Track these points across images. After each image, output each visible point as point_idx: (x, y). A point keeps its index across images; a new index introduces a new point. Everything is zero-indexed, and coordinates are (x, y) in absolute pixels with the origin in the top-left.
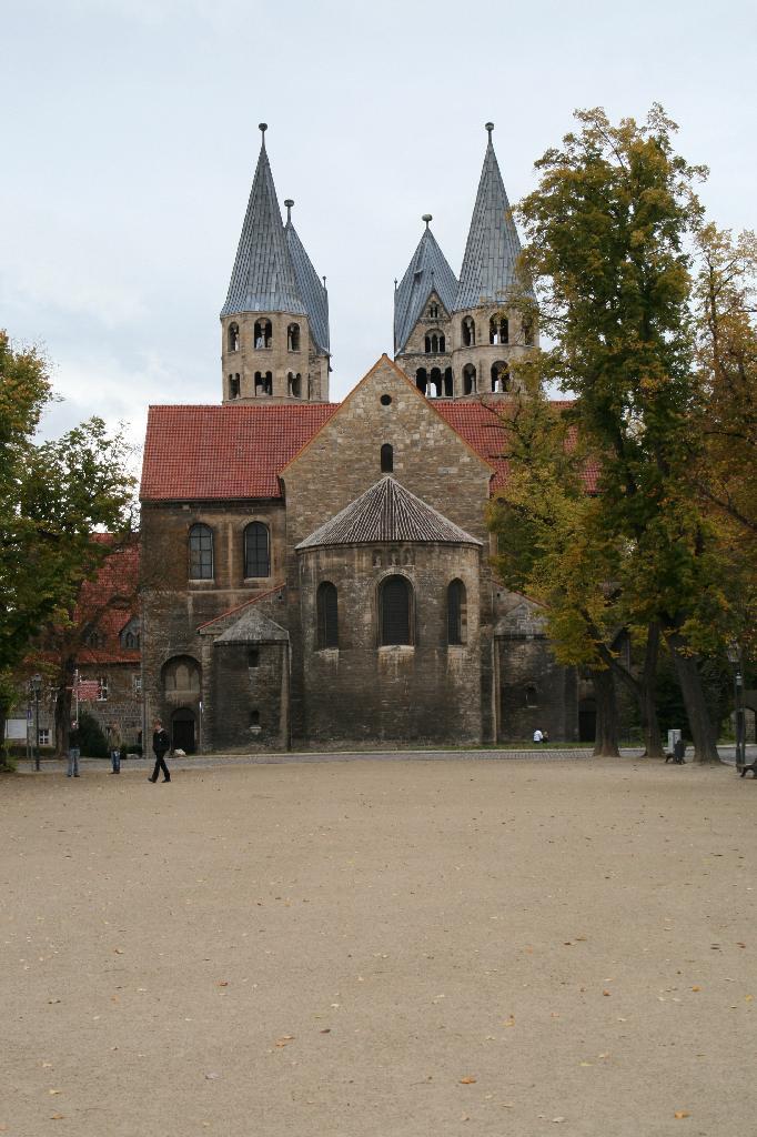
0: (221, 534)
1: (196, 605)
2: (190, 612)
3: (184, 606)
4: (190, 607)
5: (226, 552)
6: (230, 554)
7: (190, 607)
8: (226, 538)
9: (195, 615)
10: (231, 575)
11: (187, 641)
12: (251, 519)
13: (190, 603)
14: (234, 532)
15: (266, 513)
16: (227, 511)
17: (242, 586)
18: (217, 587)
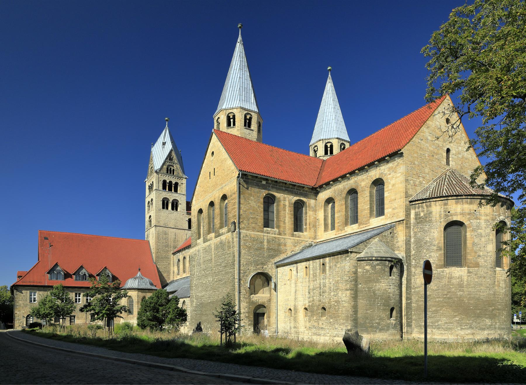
0: (282, 203)
1: (268, 242)
2: (265, 247)
3: (262, 243)
4: (265, 243)
5: (285, 214)
6: (287, 216)
7: (265, 243)
8: (285, 205)
9: (268, 249)
10: (287, 228)
11: (263, 264)
12: (296, 198)
13: (265, 241)
14: (289, 203)
15: (305, 196)
16: (286, 190)
17: (293, 235)
18: (280, 234)
